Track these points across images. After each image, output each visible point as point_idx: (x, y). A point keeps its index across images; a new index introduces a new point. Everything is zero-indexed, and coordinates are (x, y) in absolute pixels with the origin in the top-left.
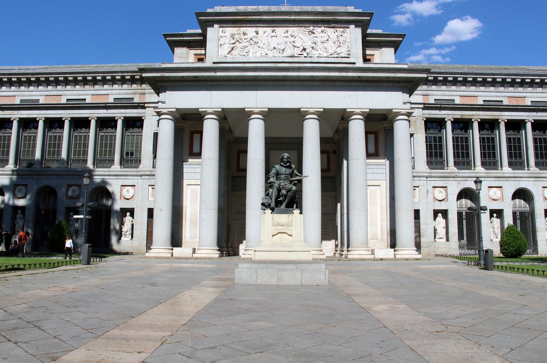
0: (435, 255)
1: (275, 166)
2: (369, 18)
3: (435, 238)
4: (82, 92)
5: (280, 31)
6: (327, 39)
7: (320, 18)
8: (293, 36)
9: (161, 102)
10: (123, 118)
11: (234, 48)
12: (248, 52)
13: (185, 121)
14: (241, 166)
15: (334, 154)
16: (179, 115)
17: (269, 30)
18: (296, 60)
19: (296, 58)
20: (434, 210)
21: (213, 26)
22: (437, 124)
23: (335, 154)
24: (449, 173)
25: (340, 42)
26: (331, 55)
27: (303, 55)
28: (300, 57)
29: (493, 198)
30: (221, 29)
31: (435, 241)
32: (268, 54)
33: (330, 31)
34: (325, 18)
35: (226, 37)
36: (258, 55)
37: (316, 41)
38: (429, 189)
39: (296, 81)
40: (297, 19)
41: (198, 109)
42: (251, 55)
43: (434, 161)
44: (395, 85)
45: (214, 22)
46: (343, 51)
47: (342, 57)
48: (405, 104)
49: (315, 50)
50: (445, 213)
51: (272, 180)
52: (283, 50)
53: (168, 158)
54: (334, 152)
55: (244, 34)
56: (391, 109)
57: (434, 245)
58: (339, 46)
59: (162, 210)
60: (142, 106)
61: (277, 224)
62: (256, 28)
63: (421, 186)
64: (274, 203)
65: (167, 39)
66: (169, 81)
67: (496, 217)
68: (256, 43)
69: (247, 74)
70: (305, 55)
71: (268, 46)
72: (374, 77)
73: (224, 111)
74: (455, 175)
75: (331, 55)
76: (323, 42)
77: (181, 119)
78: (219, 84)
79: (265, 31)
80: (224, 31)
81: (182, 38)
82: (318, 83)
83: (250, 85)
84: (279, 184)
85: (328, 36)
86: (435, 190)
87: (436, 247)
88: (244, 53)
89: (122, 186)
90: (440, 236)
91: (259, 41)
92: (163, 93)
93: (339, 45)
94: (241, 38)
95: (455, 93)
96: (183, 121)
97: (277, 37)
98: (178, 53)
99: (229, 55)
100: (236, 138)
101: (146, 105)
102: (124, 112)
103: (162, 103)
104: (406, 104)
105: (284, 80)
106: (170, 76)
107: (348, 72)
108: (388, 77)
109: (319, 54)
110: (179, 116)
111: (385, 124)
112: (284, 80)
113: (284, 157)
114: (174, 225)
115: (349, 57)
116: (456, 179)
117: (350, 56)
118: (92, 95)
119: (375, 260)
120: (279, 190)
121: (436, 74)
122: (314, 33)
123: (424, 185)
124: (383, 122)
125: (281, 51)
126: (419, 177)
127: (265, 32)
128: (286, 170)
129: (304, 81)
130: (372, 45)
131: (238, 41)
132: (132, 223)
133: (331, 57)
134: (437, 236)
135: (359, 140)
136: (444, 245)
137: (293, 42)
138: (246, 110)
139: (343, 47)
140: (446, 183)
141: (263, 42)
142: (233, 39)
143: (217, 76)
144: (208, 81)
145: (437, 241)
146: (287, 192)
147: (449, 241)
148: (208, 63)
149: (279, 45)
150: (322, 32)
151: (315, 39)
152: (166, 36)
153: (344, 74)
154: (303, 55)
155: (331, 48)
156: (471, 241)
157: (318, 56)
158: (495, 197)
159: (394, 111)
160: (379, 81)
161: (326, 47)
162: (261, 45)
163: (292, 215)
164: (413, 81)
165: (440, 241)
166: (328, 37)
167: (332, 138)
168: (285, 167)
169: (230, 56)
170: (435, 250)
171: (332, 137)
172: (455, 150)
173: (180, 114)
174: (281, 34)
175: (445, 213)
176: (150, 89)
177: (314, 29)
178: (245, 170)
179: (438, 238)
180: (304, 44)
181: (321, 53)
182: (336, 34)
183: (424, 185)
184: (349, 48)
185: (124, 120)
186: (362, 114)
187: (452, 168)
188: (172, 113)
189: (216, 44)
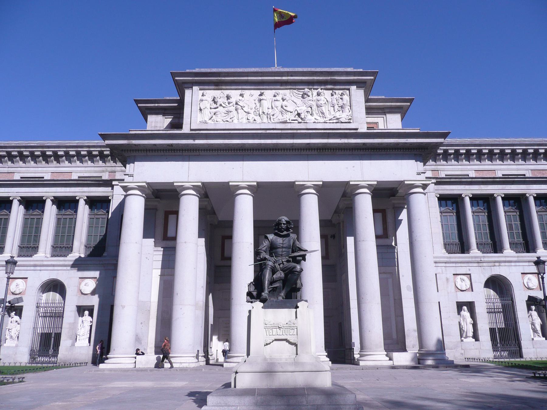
0: (465, 358)
1: (268, 235)
2: (372, 78)
3: (461, 337)
4: (40, 169)
5: (269, 94)
6: (324, 103)
7: (315, 78)
8: (285, 99)
9: (128, 175)
10: (86, 198)
11: (217, 113)
12: (233, 118)
13: (159, 199)
14: (226, 254)
15: (333, 238)
16: (151, 191)
18: (289, 126)
20: (457, 302)
21: (192, 88)
22: (452, 202)
23: (334, 239)
24: (472, 257)
25: (339, 105)
26: (330, 120)
27: (297, 120)
28: (294, 123)
29: (528, 286)
31: (462, 341)
33: (327, 94)
34: (321, 78)
35: (207, 100)
37: (312, 105)
38: (448, 277)
39: (290, 149)
40: (289, 81)
41: (173, 183)
42: (236, 121)
43: (452, 244)
44: (407, 153)
45: (193, 84)
46: (344, 116)
48: (418, 175)
49: (311, 115)
50: (471, 306)
51: (263, 255)
52: (273, 115)
53: (135, 242)
54: (333, 236)
55: (228, 97)
56: (403, 181)
57: (461, 346)
58: (339, 110)
59: (124, 307)
60: (108, 183)
61: (273, 325)
62: (241, 91)
63: (439, 273)
64: (266, 291)
65: (139, 105)
66: (138, 150)
67: (535, 310)
68: (242, 108)
69: (232, 141)
70: (300, 120)
71: (256, 111)
72: (382, 144)
73: (204, 186)
74: (479, 259)
75: (330, 120)
76: (320, 106)
77: (153, 197)
78: (198, 154)
79: (252, 94)
80: (204, 94)
81: (156, 105)
82: (316, 152)
83: (235, 155)
84: (274, 261)
85: (326, 99)
86: (457, 278)
88: (227, 120)
89: (80, 278)
91: (245, 105)
92: (131, 164)
93: (339, 109)
94: (225, 102)
95: (469, 167)
96: (156, 199)
97: (266, 100)
98: (152, 122)
99: (210, 122)
100: (220, 222)
101: (114, 183)
102: (87, 191)
103: (129, 176)
104: (420, 174)
105: (276, 150)
106: (139, 144)
108: (398, 144)
109: (315, 119)
110: (151, 193)
111: (395, 201)
112: (276, 150)
113: (282, 222)
114: (142, 325)
115: (350, 123)
116: (481, 264)
117: (351, 121)
118: (51, 172)
119: (393, 367)
120: (274, 271)
121: (446, 147)
122: (309, 96)
123: (442, 272)
124: (391, 198)
125: (271, 117)
127: (252, 95)
128: (283, 241)
129: (298, 149)
130: (376, 112)
131: (221, 105)
132: (91, 324)
134: (464, 336)
135: (366, 218)
136: (473, 345)
137: (285, 106)
138: (230, 184)
139: (344, 111)
140: (469, 269)
142: (215, 103)
143: (195, 144)
144: (185, 150)
145: (464, 341)
146: (286, 275)
147: (479, 341)
148: (186, 129)
149: (269, 110)
150: (318, 94)
151: (310, 102)
152: (137, 102)
154: (297, 120)
155: (330, 113)
156: (506, 341)
157: (314, 121)
158: (531, 285)
159: (406, 182)
160: (387, 149)
161: (324, 111)
162: (249, 110)
163: (296, 312)
164: (427, 148)
166: (325, 100)
167: (330, 221)
168: (281, 236)
170: (463, 352)
171: (330, 219)
172: (476, 231)
173: (152, 190)
175: (471, 306)
176: (121, 167)
177: (309, 92)
178: (230, 259)
180: (298, 109)
181: (318, 118)
182: (335, 96)
183: (442, 272)
184: (351, 112)
185: (88, 200)
186: (369, 187)
187: (475, 252)
188: (142, 189)
189: (196, 108)
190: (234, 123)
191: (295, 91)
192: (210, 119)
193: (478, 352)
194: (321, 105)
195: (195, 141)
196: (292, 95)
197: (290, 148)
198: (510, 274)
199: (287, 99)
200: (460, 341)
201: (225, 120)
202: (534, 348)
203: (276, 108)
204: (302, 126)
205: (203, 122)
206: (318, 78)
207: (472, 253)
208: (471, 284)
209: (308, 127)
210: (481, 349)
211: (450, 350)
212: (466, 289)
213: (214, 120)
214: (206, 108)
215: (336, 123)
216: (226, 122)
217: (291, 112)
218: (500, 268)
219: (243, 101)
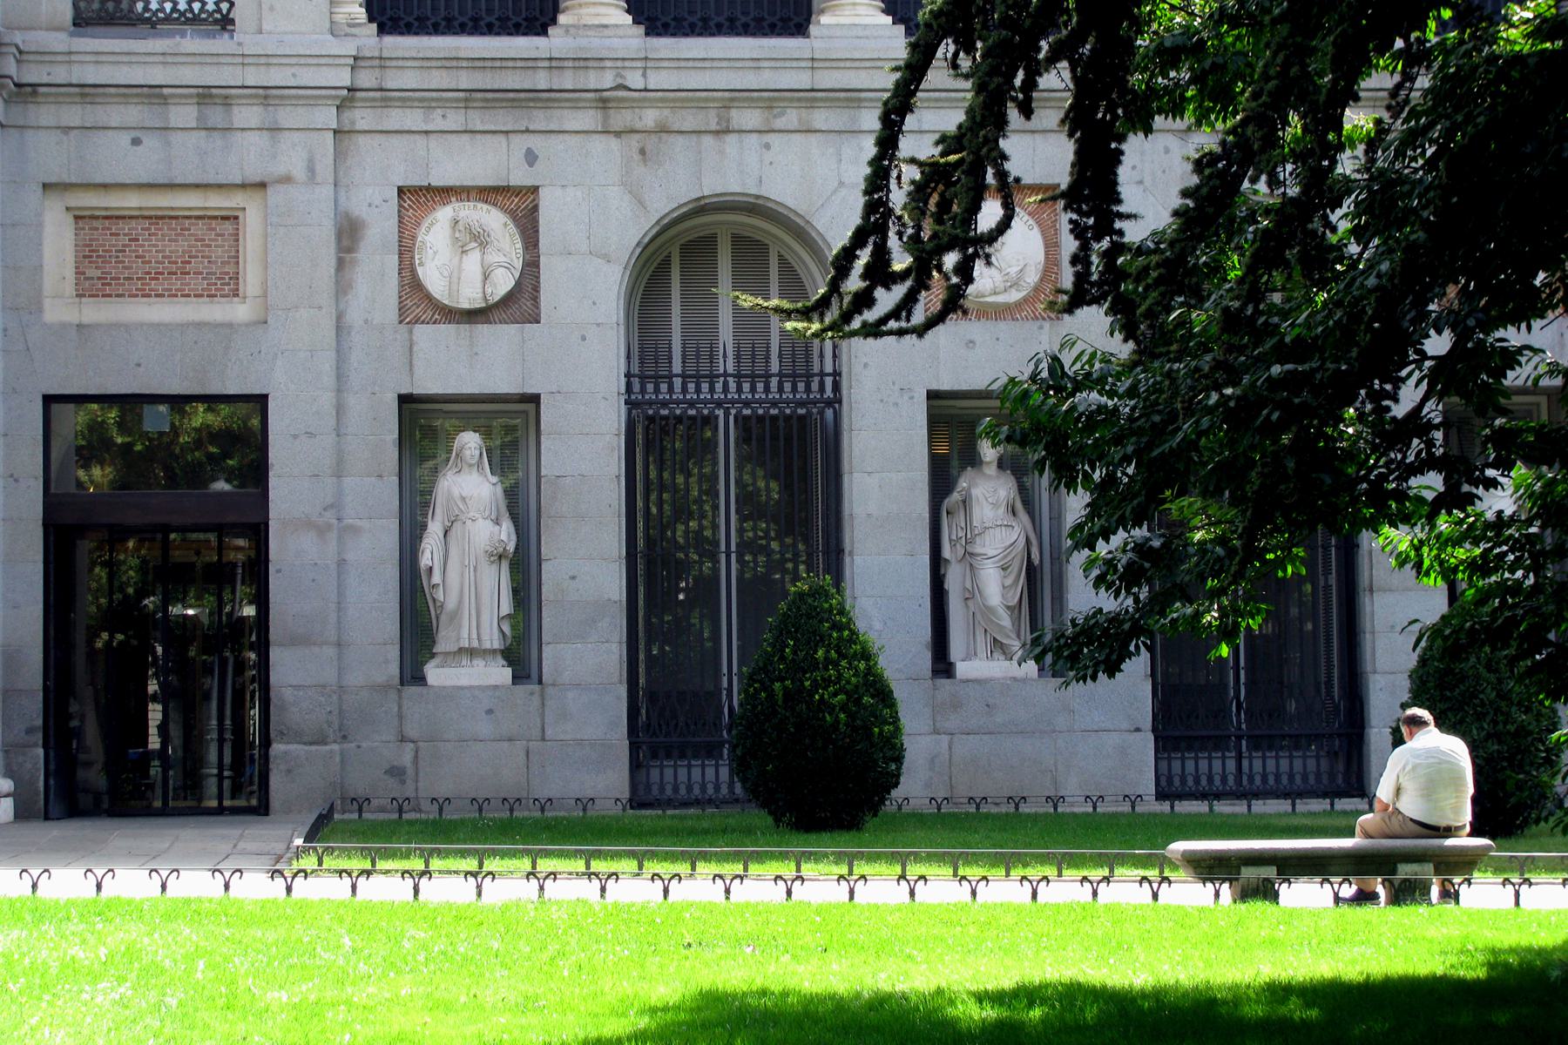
24: (555, 63)
57: (400, 717)
74: (608, 80)
86: (425, 224)
87: (411, 731)
90: (458, 640)
123: (311, 170)
126: (266, 95)
136: (490, 712)
165: (464, 682)
170: (406, 759)
179: (447, 654)
183: (311, 170)
193: (522, 755)
198: (835, 191)
200: (397, 680)
202: (936, 732)
207: (567, 28)
208: (532, 266)
210: (543, 739)
211: (306, 748)
212: (480, 304)
218: (767, 146)
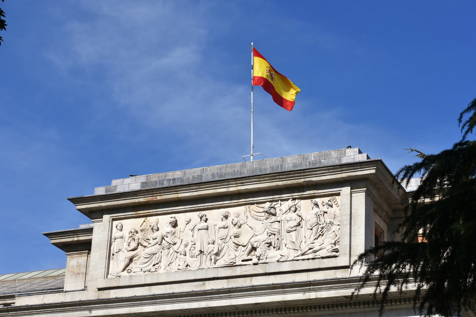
7: (280, 183)
12: (157, 264)
17: (195, 216)
18: (238, 271)
19: (239, 267)
26: (303, 255)
27: (251, 260)
28: (246, 265)
30: (115, 223)
32: (190, 265)
33: (305, 205)
36: (174, 267)
45: (103, 212)
47: (323, 258)
58: (320, 235)
69: (142, 309)
70: (255, 260)
85: (300, 216)
91: (176, 240)
97: (207, 229)
98: (73, 267)
107: (320, 290)
115: (335, 257)
117: (337, 254)
127: (188, 222)
133: (303, 260)
141: (183, 243)
153: (312, 295)
154: (251, 260)
169: (128, 274)
174: (215, 223)
190: (158, 272)
191: (253, 207)
192: (124, 270)
194: (291, 230)
195: (91, 313)
196: (249, 216)
197: (235, 311)
199: (238, 224)
201: (144, 269)
203: (220, 241)
204: (259, 270)
205: (114, 275)
206: (285, 183)
209: (268, 271)
213: (129, 271)
214: (120, 250)
215: (313, 259)
216: (146, 273)
217: (244, 246)
219: (174, 234)
